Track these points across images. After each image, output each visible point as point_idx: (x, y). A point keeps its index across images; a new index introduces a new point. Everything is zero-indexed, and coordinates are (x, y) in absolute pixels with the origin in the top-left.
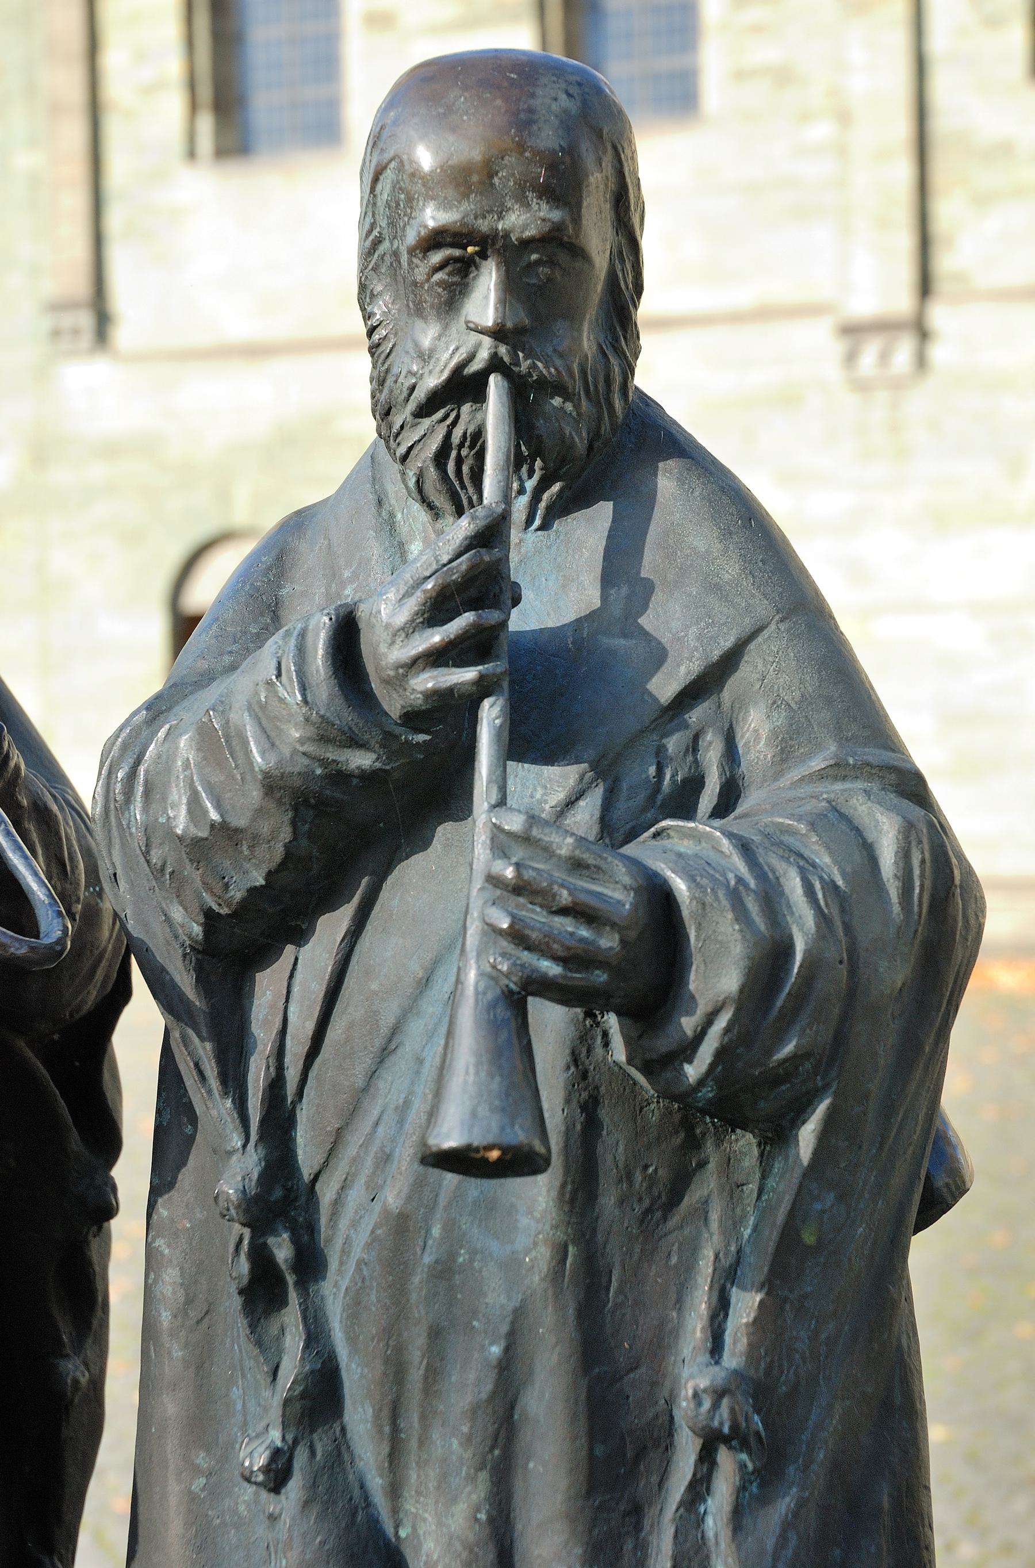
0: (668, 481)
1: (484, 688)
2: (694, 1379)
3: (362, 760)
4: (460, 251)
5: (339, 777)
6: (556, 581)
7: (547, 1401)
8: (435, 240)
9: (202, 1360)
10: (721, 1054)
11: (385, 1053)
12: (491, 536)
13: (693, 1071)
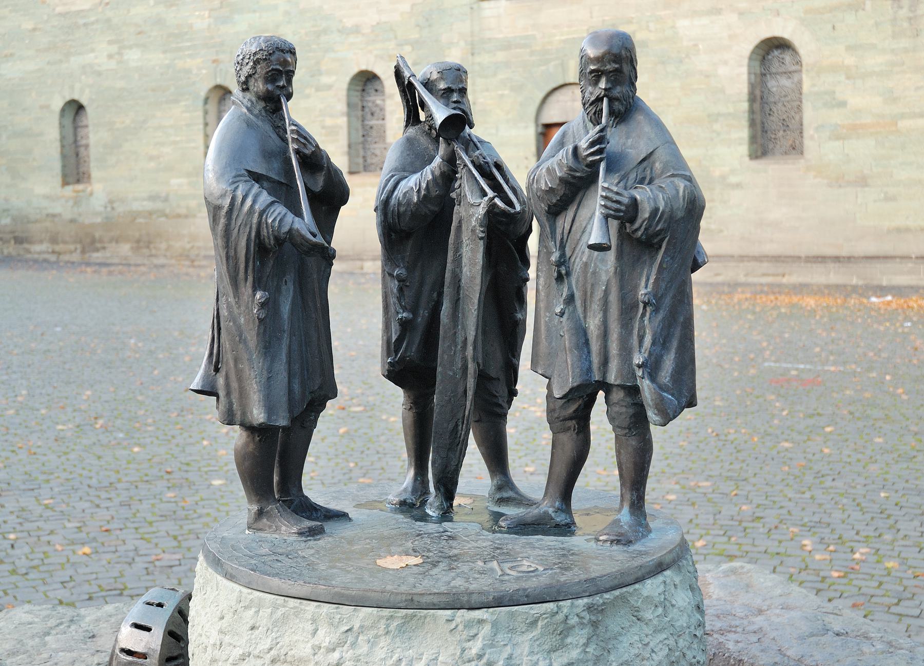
0: (640, 117)
1: (601, 160)
2: (643, 292)
3: (578, 174)
4: (597, 75)
5: (574, 177)
6: (617, 140)
7: (613, 298)
8: (592, 71)
9: (548, 296)
10: (646, 229)
11: (583, 232)
12: (602, 131)
13: (640, 233)
